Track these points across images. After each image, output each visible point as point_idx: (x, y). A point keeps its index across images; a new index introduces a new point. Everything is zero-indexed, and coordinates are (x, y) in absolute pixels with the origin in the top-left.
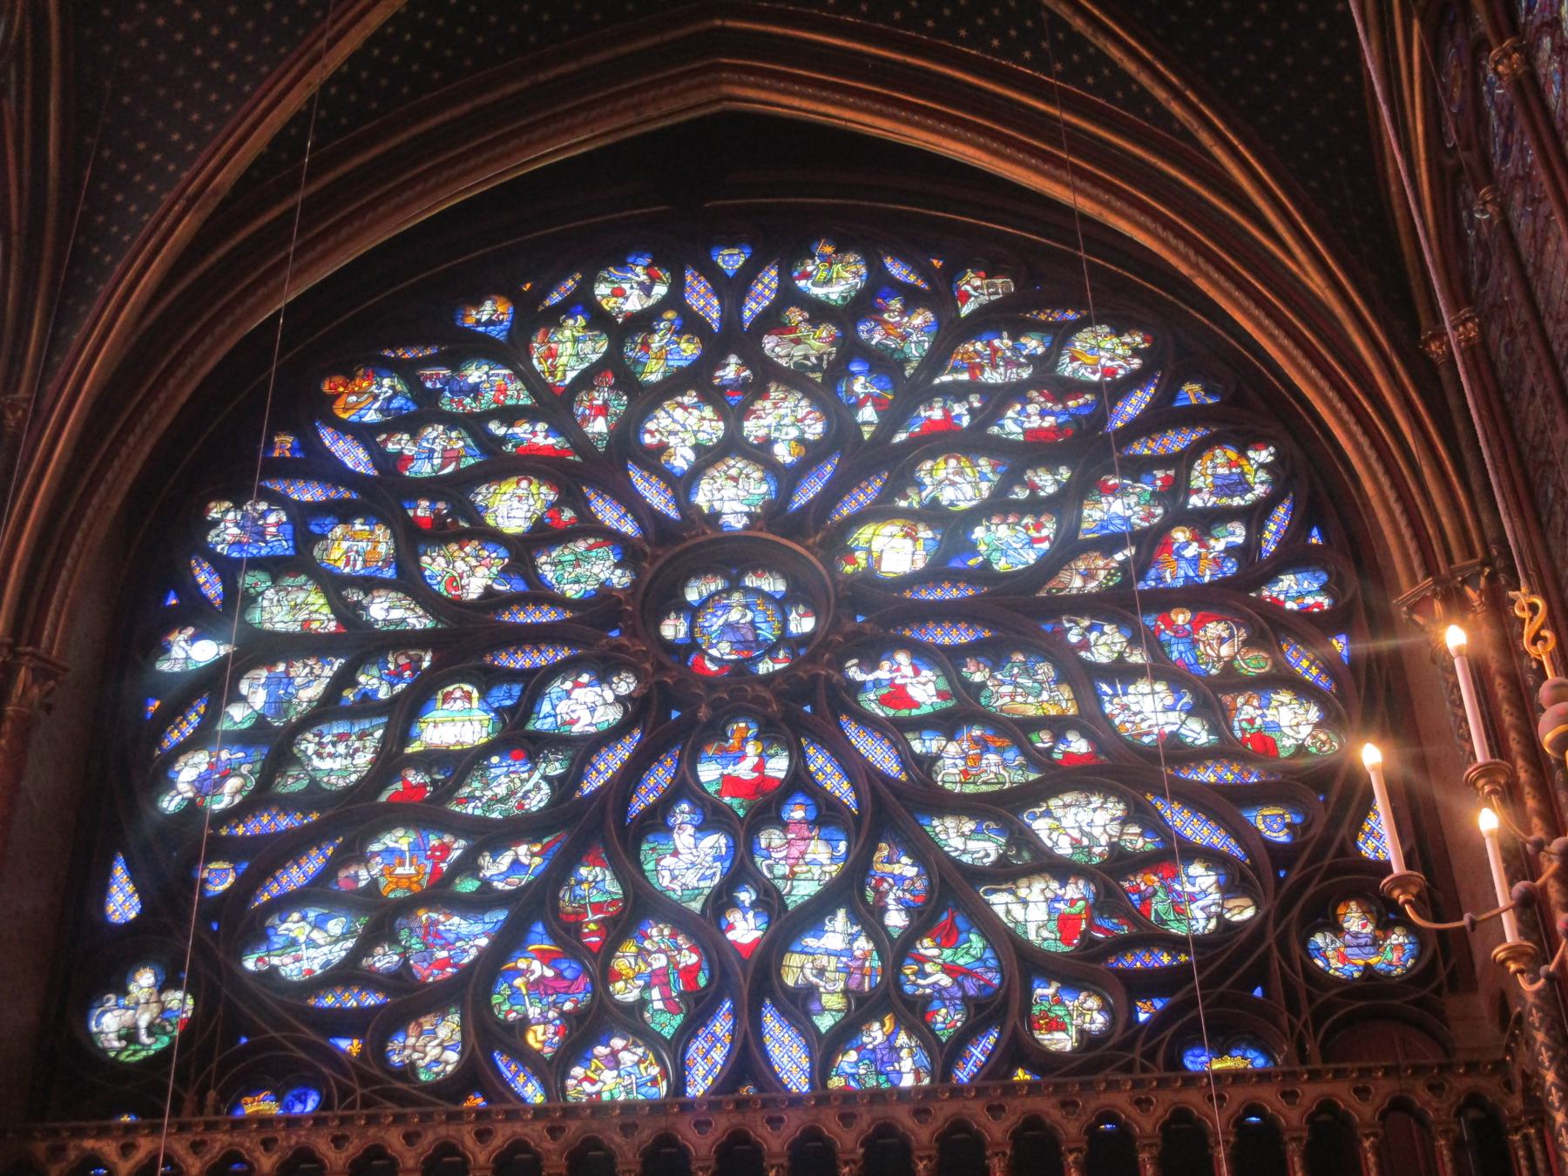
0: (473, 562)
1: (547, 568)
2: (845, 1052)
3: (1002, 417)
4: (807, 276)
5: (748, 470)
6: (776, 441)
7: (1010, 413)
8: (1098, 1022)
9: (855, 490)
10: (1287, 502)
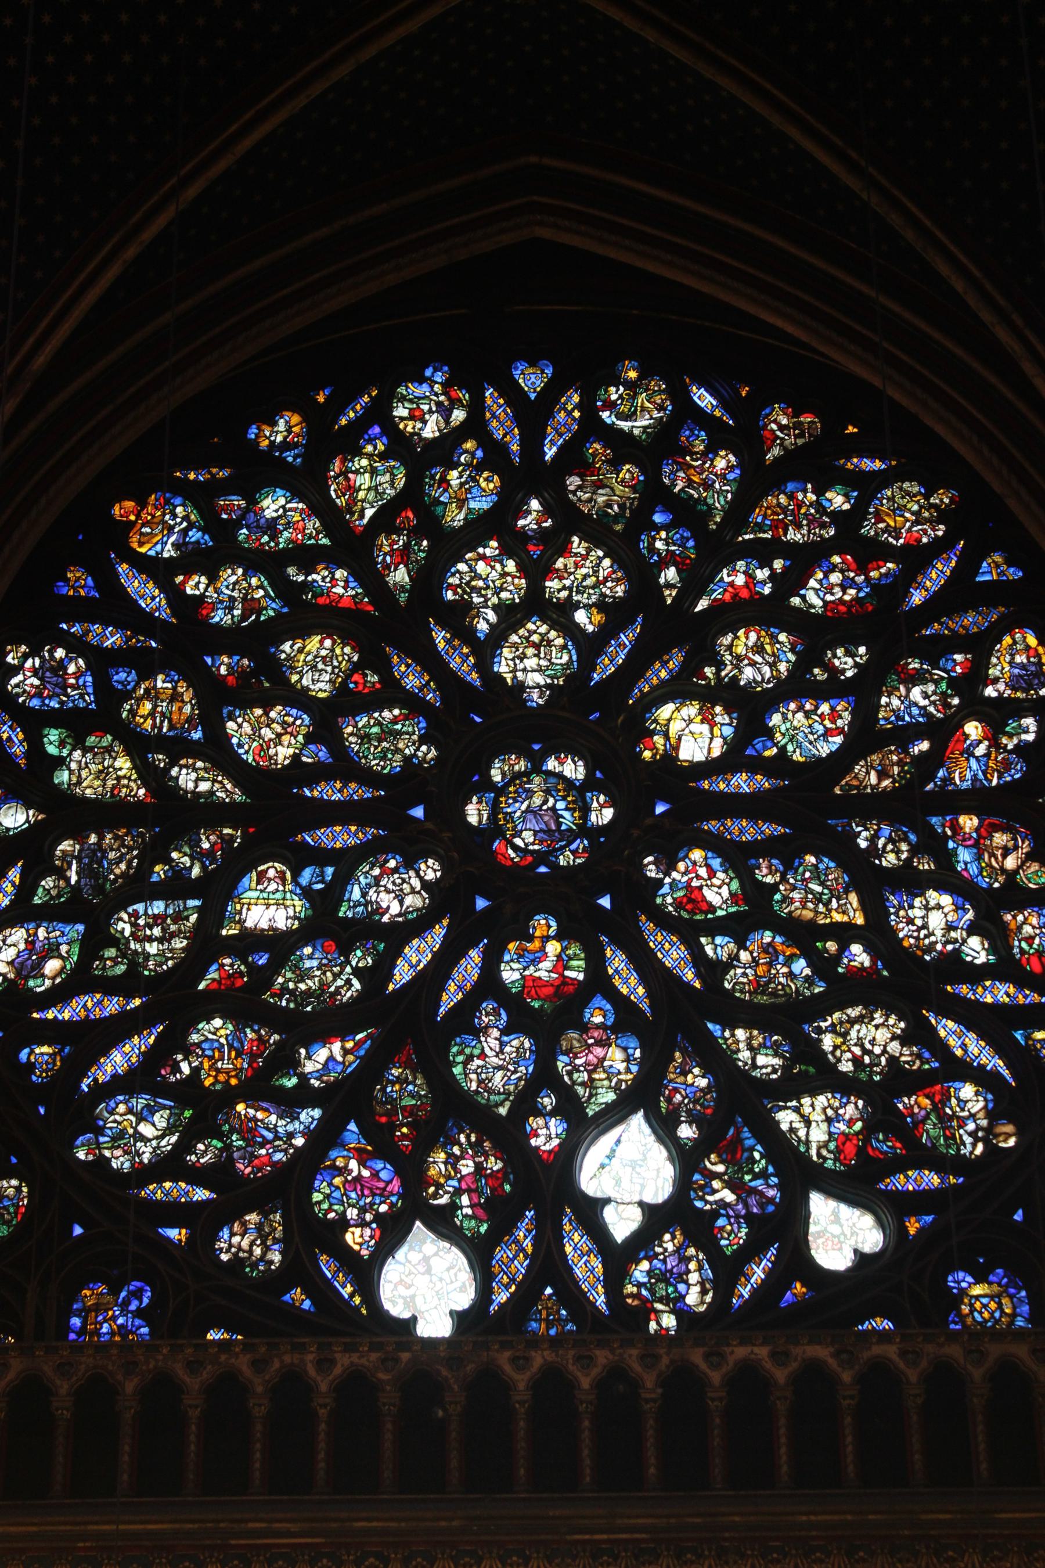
0: (279, 729)
2: (638, 1262)
3: (804, 585)
4: (610, 405)
5: (553, 634)
6: (577, 606)
7: (812, 583)
9: (657, 665)
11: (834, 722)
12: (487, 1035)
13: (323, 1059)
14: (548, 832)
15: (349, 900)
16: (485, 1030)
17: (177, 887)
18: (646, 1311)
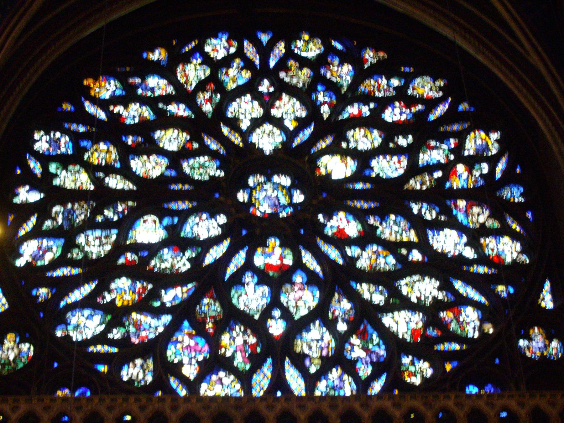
8: (429, 372)
9: (321, 141)
10: (506, 155)
13: (171, 296)
14: (275, 205)
17: (107, 225)
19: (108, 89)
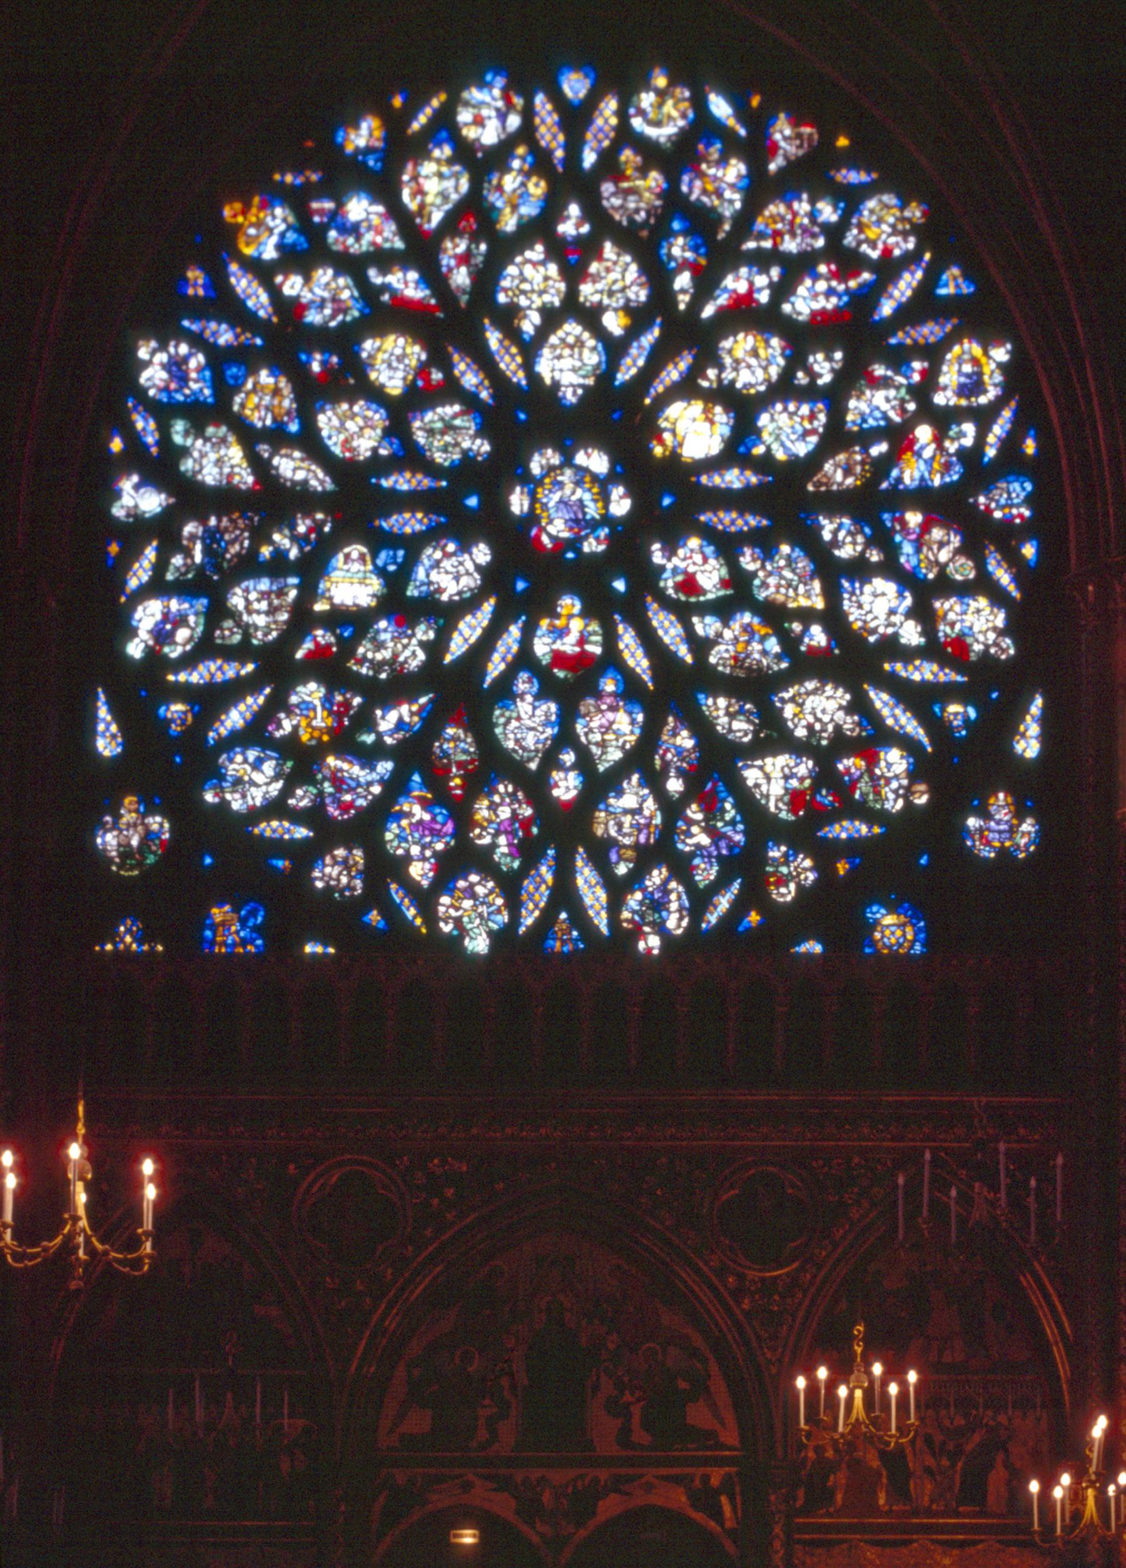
1: (420, 433)
2: (632, 892)
3: (793, 292)
5: (586, 335)
7: (801, 290)
11: (811, 422)
12: (523, 700)
14: (576, 521)
15: (415, 580)
16: (522, 696)
18: (637, 932)
19: (268, 231)
